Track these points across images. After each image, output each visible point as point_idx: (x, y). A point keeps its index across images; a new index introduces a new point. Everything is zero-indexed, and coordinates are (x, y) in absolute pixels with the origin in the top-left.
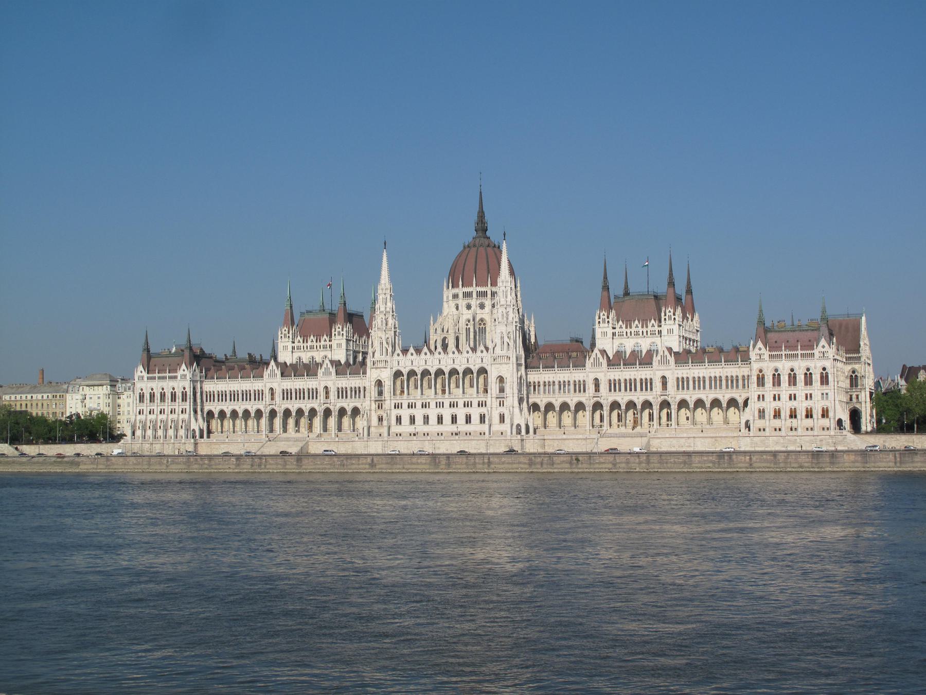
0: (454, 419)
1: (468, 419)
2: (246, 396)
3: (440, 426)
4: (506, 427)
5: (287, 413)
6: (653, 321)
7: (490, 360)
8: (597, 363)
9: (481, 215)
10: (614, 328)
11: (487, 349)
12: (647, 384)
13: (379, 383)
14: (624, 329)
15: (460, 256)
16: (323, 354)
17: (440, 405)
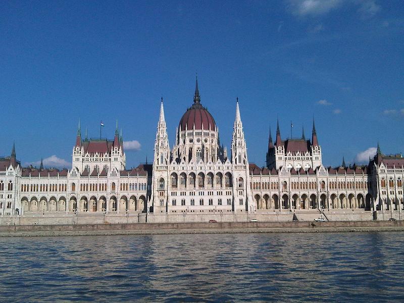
0: (211, 202)
1: (220, 202)
2: (53, 188)
3: (202, 206)
4: (243, 207)
5: (85, 198)
6: (307, 152)
7: (234, 167)
8: (285, 174)
9: (197, 93)
10: (286, 155)
11: (232, 162)
12: (314, 185)
13: (162, 180)
14: (292, 157)
15: (185, 114)
16: (105, 164)
17: (202, 194)
